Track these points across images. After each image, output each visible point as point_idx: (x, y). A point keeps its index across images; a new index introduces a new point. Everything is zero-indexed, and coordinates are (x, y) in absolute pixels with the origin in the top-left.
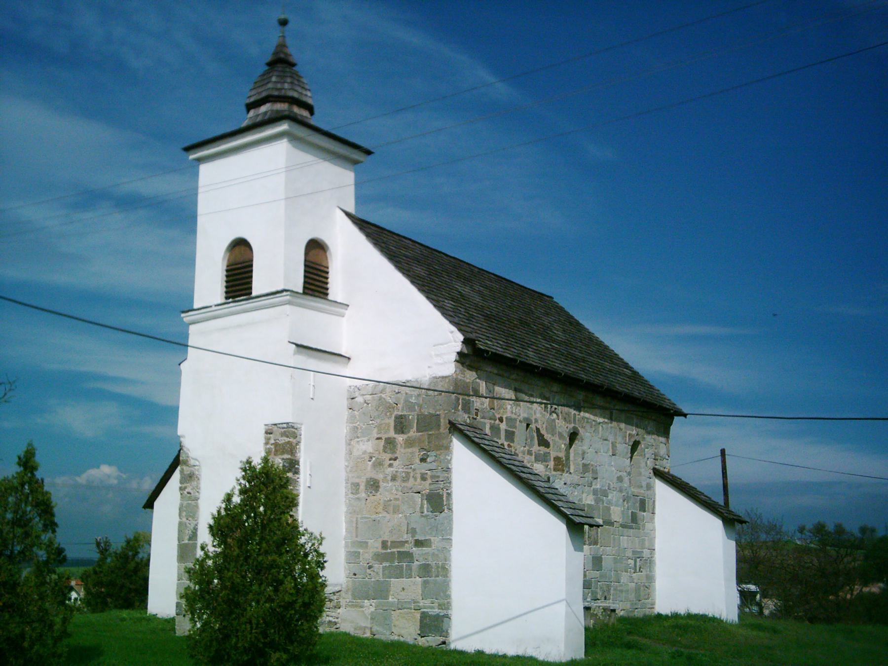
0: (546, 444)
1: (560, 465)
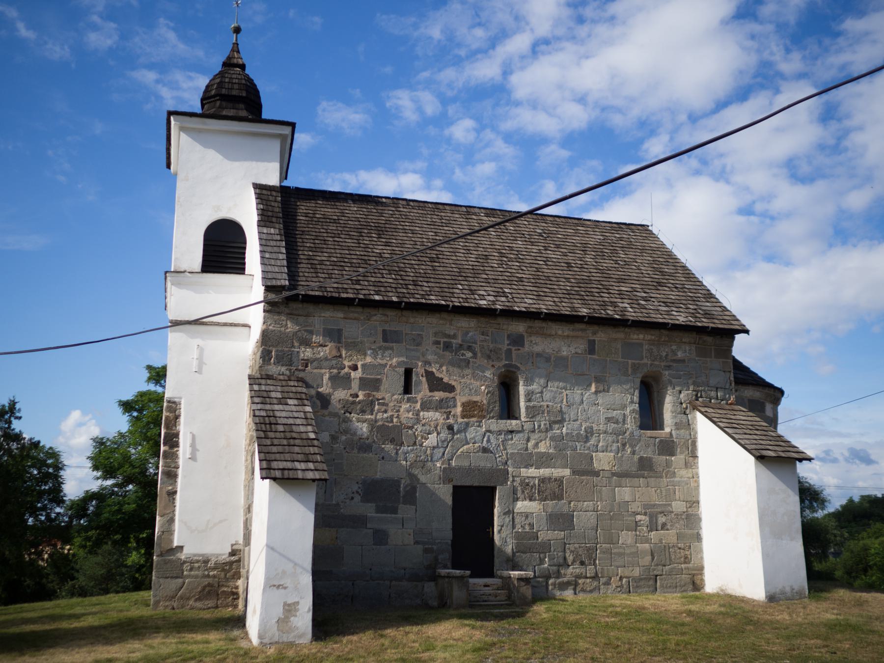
0: (450, 388)
1: (474, 411)
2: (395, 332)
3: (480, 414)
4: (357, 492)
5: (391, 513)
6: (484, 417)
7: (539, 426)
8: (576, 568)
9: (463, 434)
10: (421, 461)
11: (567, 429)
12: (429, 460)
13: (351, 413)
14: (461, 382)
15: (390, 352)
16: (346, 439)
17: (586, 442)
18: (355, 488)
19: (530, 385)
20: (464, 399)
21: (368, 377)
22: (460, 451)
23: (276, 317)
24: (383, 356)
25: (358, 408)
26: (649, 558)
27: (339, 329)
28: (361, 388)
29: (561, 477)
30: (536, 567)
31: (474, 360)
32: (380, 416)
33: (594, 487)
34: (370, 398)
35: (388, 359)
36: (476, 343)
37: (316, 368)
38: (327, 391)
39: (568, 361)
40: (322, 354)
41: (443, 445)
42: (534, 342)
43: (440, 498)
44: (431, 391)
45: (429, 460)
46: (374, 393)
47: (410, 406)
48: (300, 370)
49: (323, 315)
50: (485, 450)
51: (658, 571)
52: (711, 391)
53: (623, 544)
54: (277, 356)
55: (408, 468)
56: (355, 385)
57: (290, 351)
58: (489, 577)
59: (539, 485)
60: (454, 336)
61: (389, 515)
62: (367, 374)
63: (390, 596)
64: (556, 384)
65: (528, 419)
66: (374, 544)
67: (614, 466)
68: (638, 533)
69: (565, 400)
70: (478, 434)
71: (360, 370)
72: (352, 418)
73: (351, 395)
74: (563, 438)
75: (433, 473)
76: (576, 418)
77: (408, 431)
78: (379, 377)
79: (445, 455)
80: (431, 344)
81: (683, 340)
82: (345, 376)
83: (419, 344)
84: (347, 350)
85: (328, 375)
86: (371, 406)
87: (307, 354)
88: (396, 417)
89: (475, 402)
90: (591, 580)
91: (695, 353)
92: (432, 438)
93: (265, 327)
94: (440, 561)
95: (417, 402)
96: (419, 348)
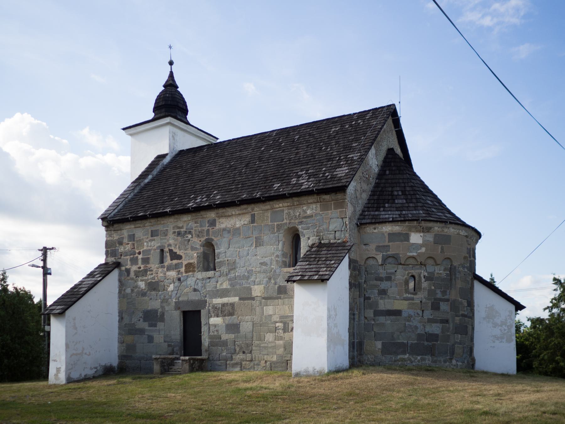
0: (179, 257)
1: (190, 268)
2: (156, 230)
4: (141, 317)
5: (155, 327)
8: (241, 355)
11: (238, 273)
15: (154, 242)
21: (145, 257)
26: (282, 349)
28: (142, 264)
36: (192, 229)
42: (221, 222)
44: (171, 260)
46: (147, 265)
50: (195, 290)
51: (287, 357)
52: (330, 234)
56: (140, 262)
59: (222, 308)
60: (182, 227)
61: (154, 328)
67: (264, 293)
68: (276, 334)
69: (238, 256)
76: (244, 265)
78: (149, 256)
81: (309, 201)
83: (166, 235)
91: (319, 209)
95: (165, 267)
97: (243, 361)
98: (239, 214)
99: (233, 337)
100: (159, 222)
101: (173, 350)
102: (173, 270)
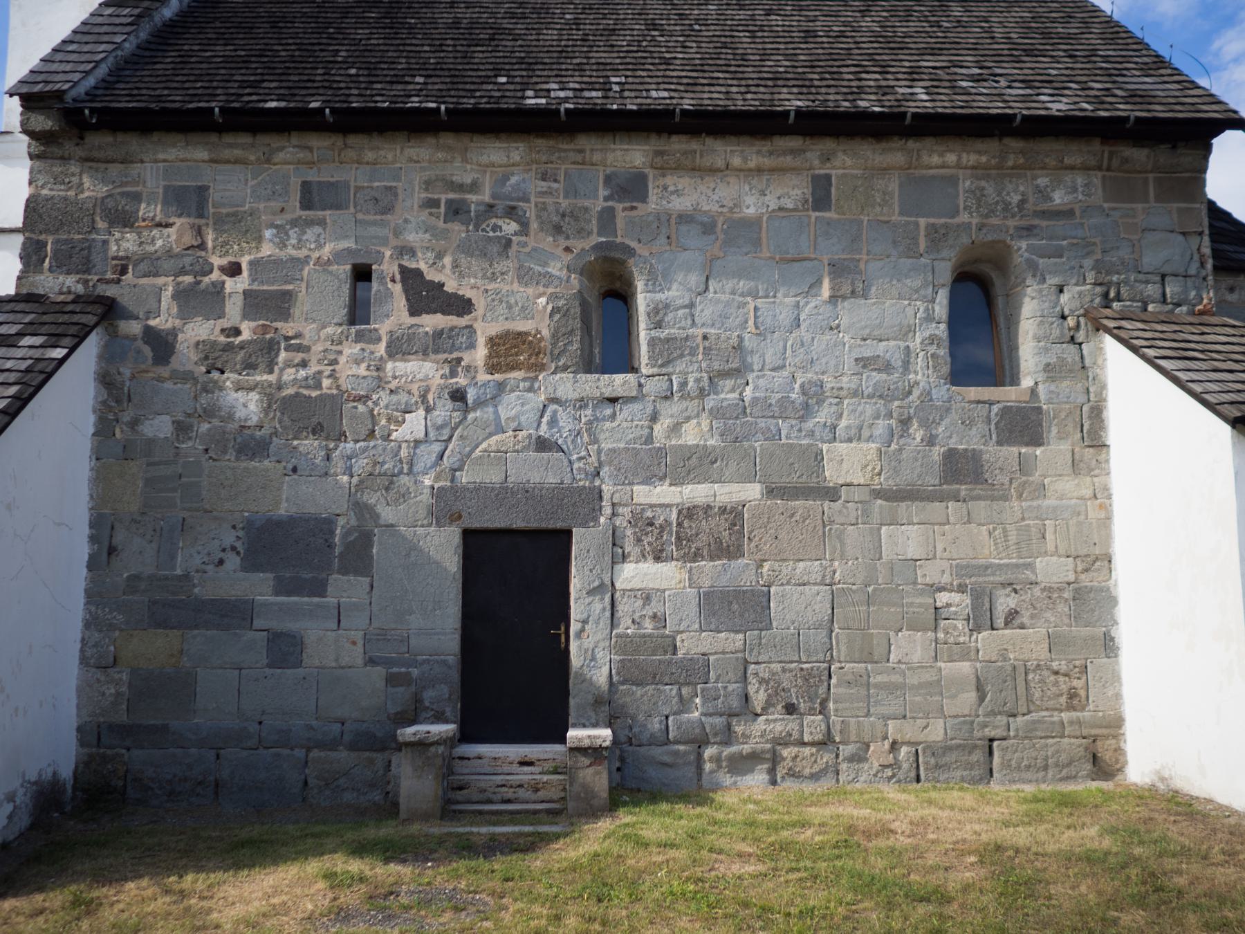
0: (462, 306)
1: (517, 354)
2: (332, 184)
3: (533, 360)
4: (233, 548)
5: (312, 594)
6: (542, 368)
7: (684, 384)
8: (775, 721)
9: (491, 409)
10: (385, 474)
12: (405, 471)
13: (223, 372)
14: (487, 291)
15: (317, 229)
16: (209, 430)
17: (803, 419)
18: (229, 538)
19: (662, 290)
20: (494, 329)
21: (265, 288)
22: (480, 448)
23: (57, 169)
24: (300, 240)
25: (239, 358)
26: (971, 696)
27: (200, 187)
28: (246, 316)
29: (738, 503)
30: (671, 719)
31: (524, 238)
32: (290, 374)
33: (824, 527)
34: (268, 336)
35: (313, 246)
37: (144, 276)
38: (169, 325)
39: (760, 229)
40: (159, 243)
41: (446, 436)
42: (671, 188)
43: (429, 558)
44: (413, 312)
45: (405, 471)
46: (278, 325)
47: (363, 350)
48: (108, 282)
49: (161, 156)
50: (543, 445)
51: (995, 727)
52: (1147, 282)
53: (899, 662)
54: (56, 252)
55: (353, 490)
56: (233, 310)
57: (87, 240)
58: (554, 743)
59: (679, 524)
60: (474, 187)
61: (306, 599)
62: (262, 283)
63: (306, 783)
64: (729, 285)
65: (655, 370)
66: (269, 666)
67: (879, 474)
68: (941, 635)
69: (751, 323)
70: (525, 408)
71: (245, 273)
72: (224, 382)
73: (223, 330)
74: (745, 413)
75: (412, 501)
76: (780, 362)
77: (356, 407)
78: (290, 287)
79: (445, 458)
80: (416, 206)
81: (1067, 161)
82: (211, 289)
83: (388, 210)
84: (218, 230)
85: (171, 288)
86: (269, 353)
87: (125, 245)
88: (329, 377)
89: (520, 334)
90: (814, 750)
91: (1100, 191)
92: (412, 422)
93: (32, 191)
94: (427, 704)
95: (379, 339)
96: (389, 217)
97: (786, 745)
98: (759, 170)
99: (739, 644)
100: (351, 154)
101: (417, 700)
102: (425, 353)
